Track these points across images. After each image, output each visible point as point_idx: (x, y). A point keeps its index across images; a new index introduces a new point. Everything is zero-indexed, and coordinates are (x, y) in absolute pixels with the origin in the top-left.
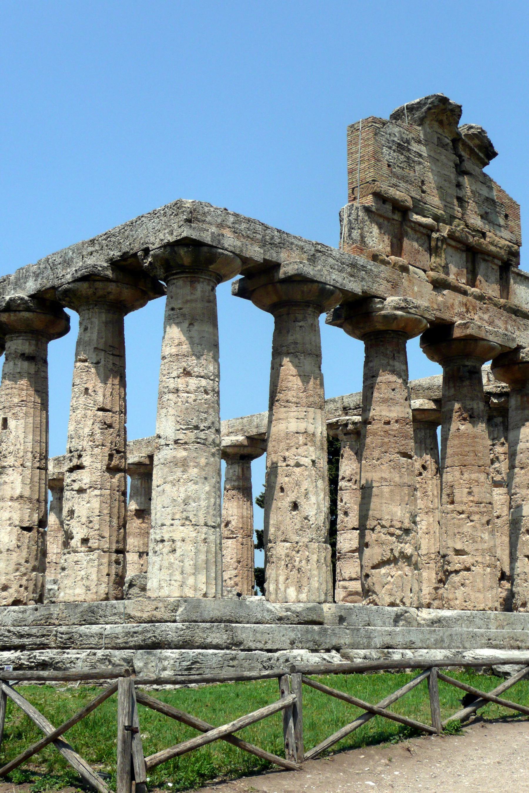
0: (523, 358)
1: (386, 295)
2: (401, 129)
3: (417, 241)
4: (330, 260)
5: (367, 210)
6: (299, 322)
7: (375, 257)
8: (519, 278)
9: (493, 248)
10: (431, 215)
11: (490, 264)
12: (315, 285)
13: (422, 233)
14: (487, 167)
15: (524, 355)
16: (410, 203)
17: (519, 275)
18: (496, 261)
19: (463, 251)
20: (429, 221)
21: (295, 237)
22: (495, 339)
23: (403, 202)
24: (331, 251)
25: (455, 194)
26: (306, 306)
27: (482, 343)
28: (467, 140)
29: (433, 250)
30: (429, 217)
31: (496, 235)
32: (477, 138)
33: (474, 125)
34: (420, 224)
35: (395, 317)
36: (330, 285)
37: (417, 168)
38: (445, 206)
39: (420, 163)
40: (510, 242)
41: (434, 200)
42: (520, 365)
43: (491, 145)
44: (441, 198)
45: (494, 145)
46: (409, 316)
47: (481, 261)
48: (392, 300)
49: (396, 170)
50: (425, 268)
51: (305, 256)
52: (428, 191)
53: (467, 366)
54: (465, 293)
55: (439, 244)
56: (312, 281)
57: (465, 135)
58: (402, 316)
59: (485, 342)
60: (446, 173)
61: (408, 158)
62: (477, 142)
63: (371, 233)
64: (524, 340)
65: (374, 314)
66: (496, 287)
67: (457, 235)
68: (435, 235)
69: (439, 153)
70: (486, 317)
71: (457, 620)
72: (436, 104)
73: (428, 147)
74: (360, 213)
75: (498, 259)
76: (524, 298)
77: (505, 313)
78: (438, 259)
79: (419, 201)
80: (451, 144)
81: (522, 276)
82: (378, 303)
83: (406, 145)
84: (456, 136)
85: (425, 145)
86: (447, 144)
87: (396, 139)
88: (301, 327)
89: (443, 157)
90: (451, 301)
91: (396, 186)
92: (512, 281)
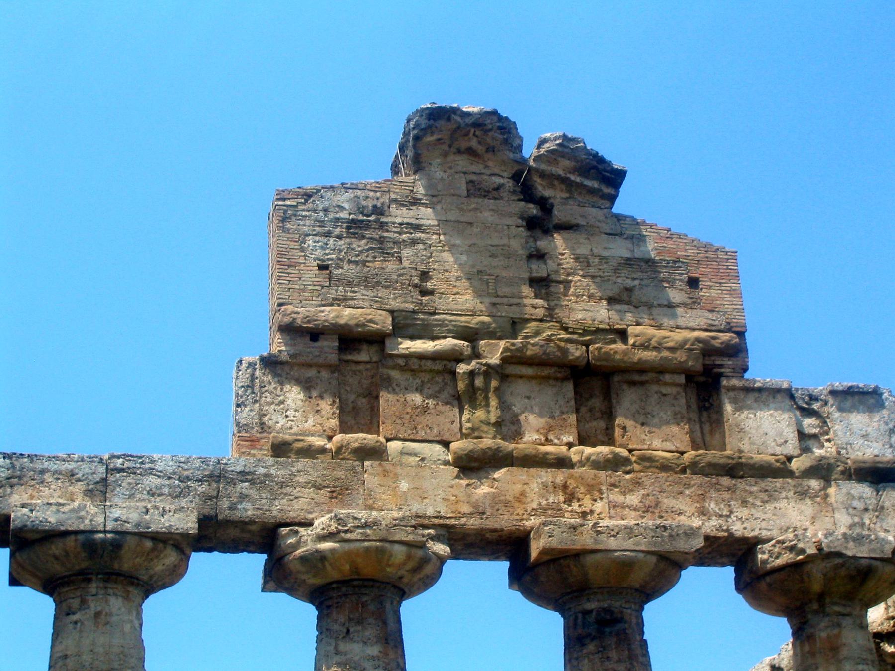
0: (764, 562)
1: (311, 516)
2: (359, 193)
3: (419, 390)
4: (152, 481)
5: (270, 363)
6: (74, 614)
7: (281, 449)
8: (751, 397)
9: (649, 355)
10: (449, 331)
11: (655, 388)
12: (70, 541)
13: (431, 371)
14: (618, 201)
15: (765, 556)
16: (385, 322)
17: (749, 390)
18: (668, 377)
19: (564, 379)
20: (449, 343)
21: (49, 459)
22: (629, 544)
23: (364, 325)
24: (152, 462)
25: (526, 275)
26: (84, 580)
27: (590, 559)
28: (544, 167)
29: (464, 399)
30: (445, 338)
31: (659, 327)
32: (563, 155)
33: (548, 135)
34: (421, 357)
35: (321, 557)
36: (105, 532)
37: (407, 252)
38: (494, 304)
39: (414, 242)
40: (706, 330)
41: (460, 301)
42: (768, 579)
43: (602, 160)
44: (478, 294)
45: (608, 157)
46: (346, 546)
47: (625, 387)
48: (322, 522)
49: (348, 271)
50: (446, 437)
51: (79, 488)
52: (443, 287)
53: (591, 612)
54: (562, 463)
55: (479, 382)
56: (66, 534)
57: (537, 158)
58: (332, 550)
59: (598, 556)
60: (496, 241)
61: (382, 240)
62: (567, 163)
63: (282, 402)
64: (764, 525)
65: (286, 559)
66: (675, 429)
67: (529, 353)
68: (462, 368)
69: (476, 209)
70: (633, 499)
72: (423, 126)
73: (438, 207)
74: (258, 373)
75: (674, 371)
76: (772, 433)
77: (697, 479)
78: (480, 414)
79: (414, 312)
80: (509, 184)
81: (760, 390)
82: (288, 535)
83: (372, 218)
84: (516, 168)
85: (432, 206)
86: (497, 189)
87: (343, 215)
88: (76, 623)
89: (487, 214)
90: (518, 487)
91: (345, 299)
92: (729, 408)
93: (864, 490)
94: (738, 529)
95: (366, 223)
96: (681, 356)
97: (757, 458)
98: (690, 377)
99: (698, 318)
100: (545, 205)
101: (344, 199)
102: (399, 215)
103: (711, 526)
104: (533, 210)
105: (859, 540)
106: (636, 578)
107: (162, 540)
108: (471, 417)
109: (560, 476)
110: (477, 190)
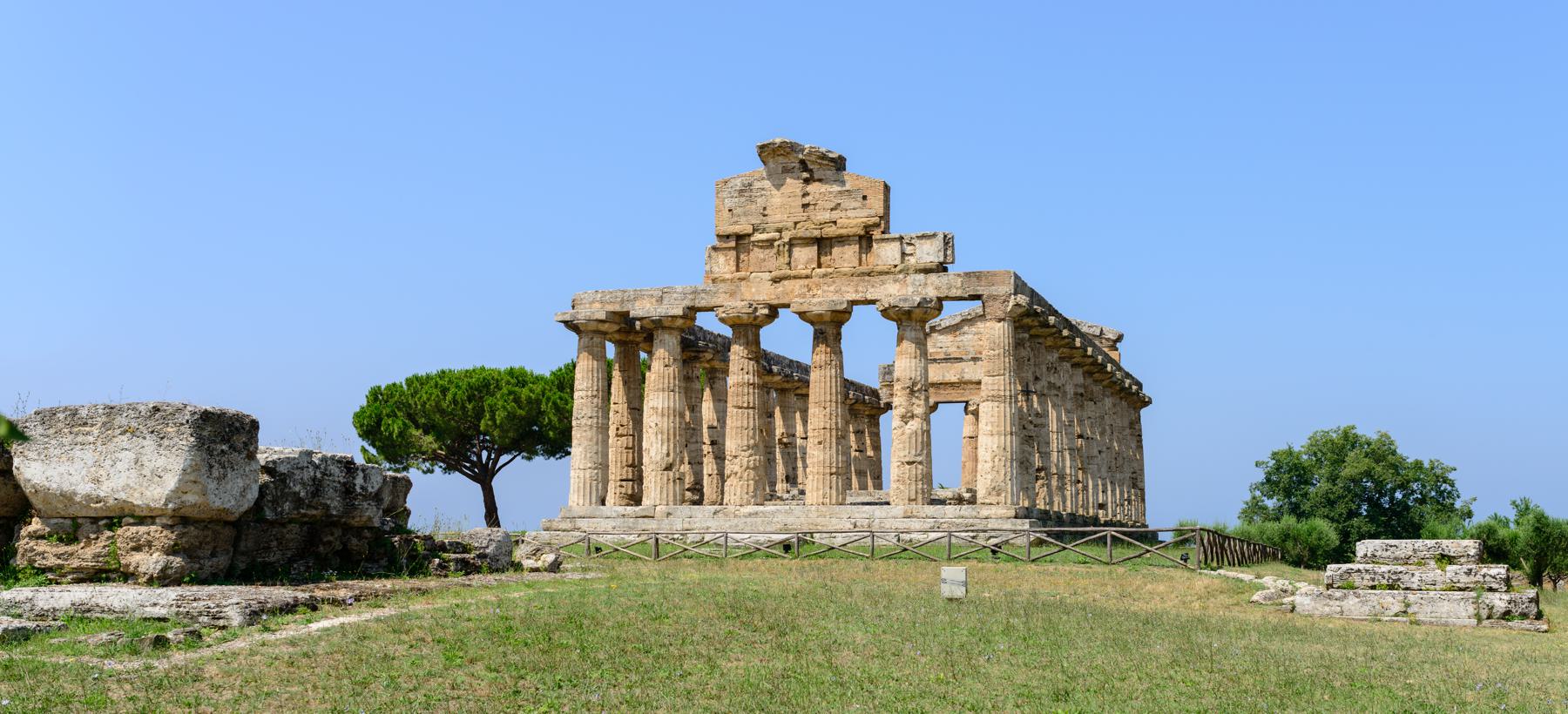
7: (714, 281)
16: (749, 230)
49: (739, 211)
54: (807, 277)
71: (773, 513)
93: (922, 276)
94: (869, 297)
95: (745, 190)
96: (854, 231)
97: (879, 268)
98: (861, 237)
99: (865, 212)
100: (810, 171)
101: (738, 182)
102: (757, 185)
103: (858, 297)
104: (805, 175)
105: (905, 300)
106: (827, 318)
107: (674, 317)
108: (784, 259)
109: (806, 282)
110: (787, 171)
